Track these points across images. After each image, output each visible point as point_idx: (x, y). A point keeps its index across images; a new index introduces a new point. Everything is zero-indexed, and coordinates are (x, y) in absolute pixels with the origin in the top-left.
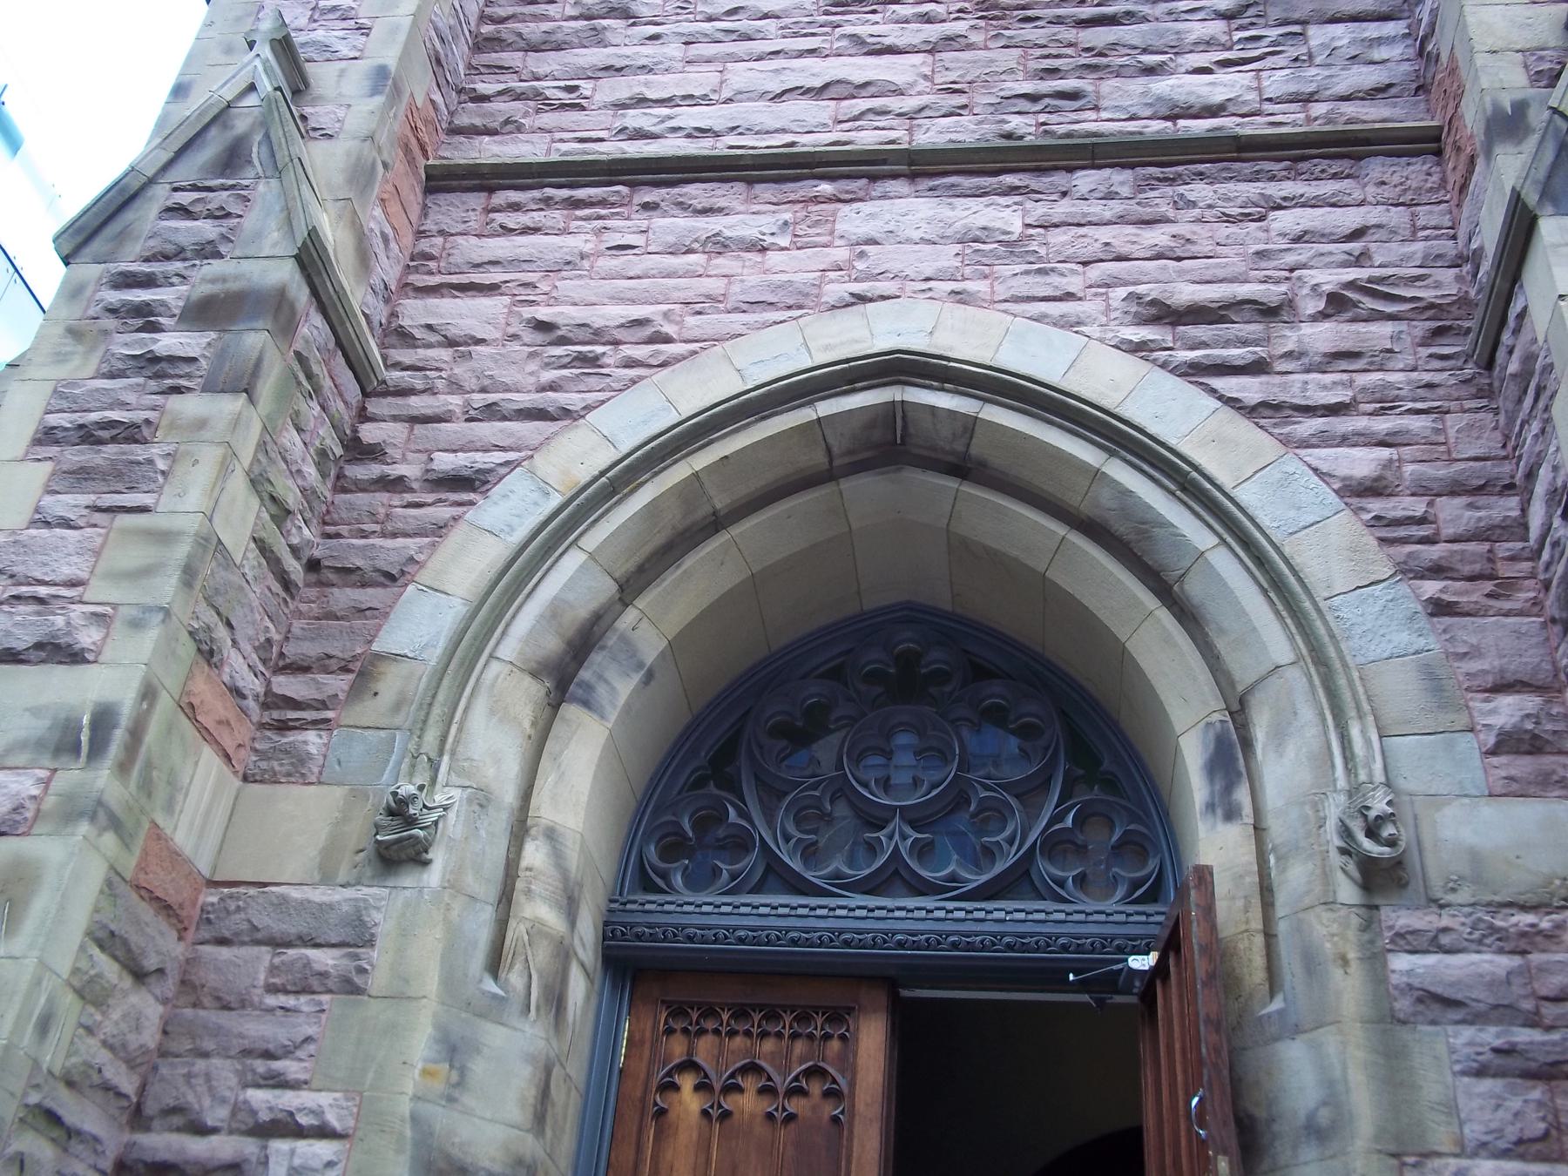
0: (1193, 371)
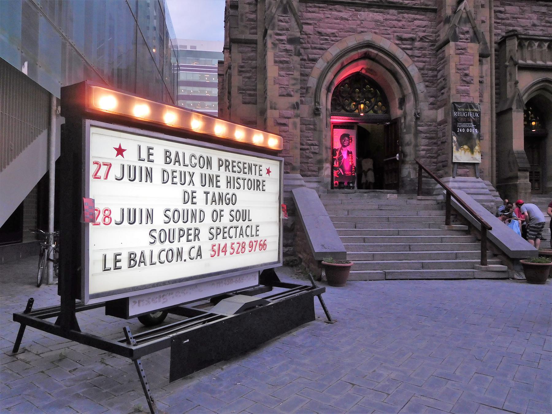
0: (403, 49)
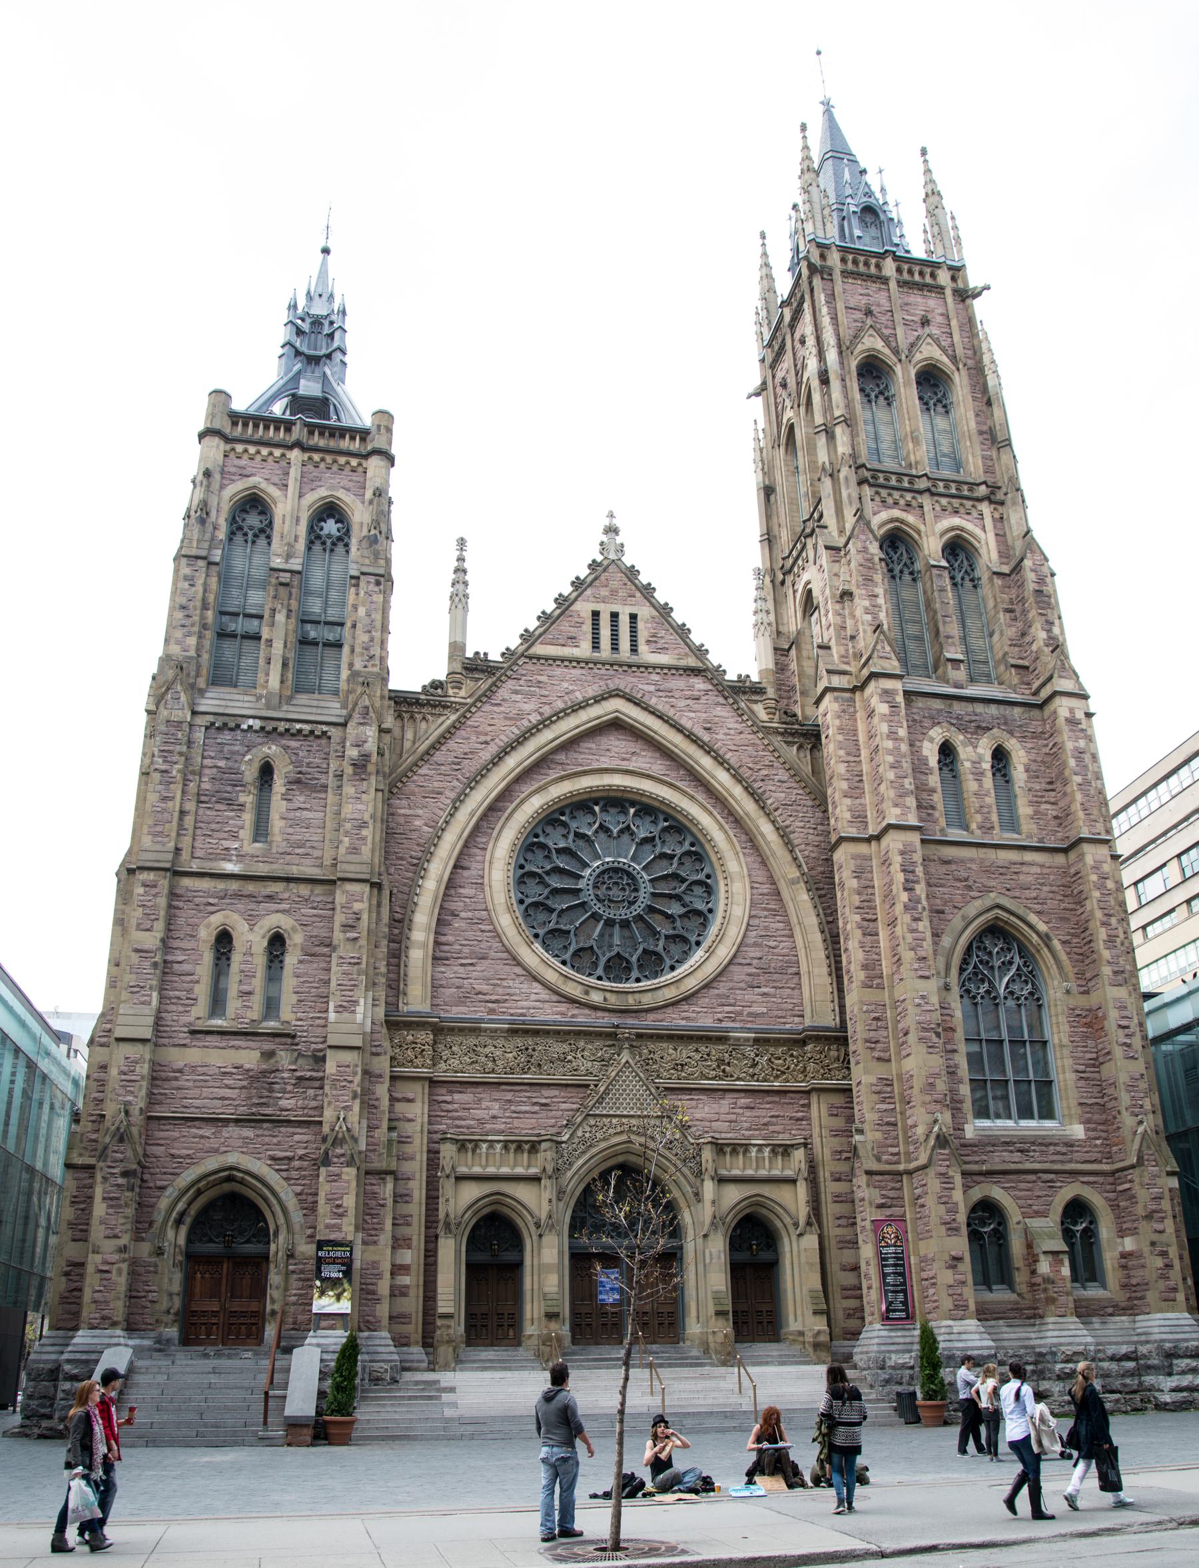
0: (277, 1170)
